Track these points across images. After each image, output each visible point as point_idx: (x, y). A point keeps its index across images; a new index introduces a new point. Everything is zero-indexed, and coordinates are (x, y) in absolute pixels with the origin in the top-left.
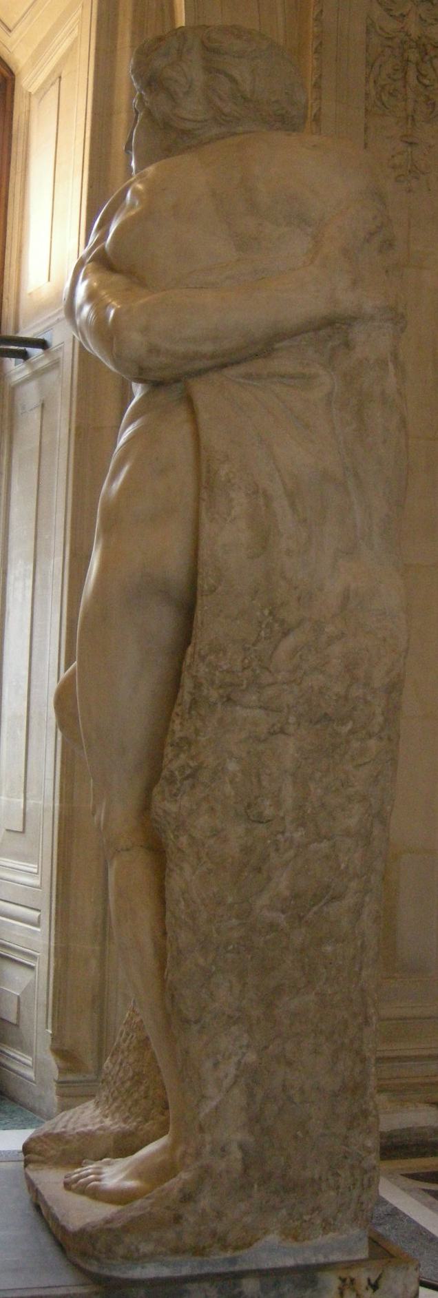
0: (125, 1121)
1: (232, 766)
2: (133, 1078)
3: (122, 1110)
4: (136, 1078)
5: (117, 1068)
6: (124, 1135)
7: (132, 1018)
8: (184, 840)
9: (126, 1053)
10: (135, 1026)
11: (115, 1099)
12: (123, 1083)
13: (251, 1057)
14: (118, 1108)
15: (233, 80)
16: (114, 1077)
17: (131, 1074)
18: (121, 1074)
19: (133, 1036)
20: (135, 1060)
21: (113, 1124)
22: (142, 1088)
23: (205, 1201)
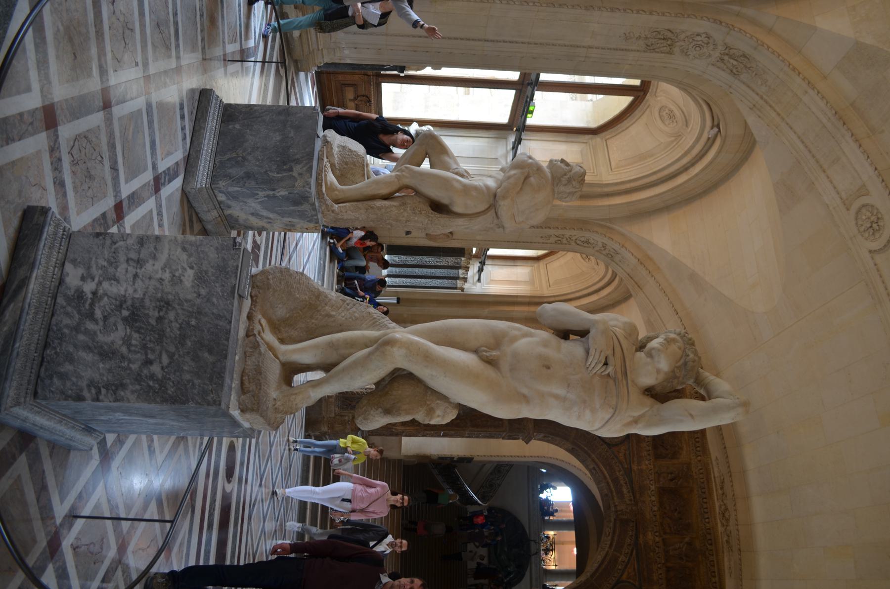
1: (416, 218)
6: (335, 166)
8: (402, 211)
13: (361, 219)
15: (566, 198)
21: (336, 160)
22: (345, 166)
23: (333, 214)
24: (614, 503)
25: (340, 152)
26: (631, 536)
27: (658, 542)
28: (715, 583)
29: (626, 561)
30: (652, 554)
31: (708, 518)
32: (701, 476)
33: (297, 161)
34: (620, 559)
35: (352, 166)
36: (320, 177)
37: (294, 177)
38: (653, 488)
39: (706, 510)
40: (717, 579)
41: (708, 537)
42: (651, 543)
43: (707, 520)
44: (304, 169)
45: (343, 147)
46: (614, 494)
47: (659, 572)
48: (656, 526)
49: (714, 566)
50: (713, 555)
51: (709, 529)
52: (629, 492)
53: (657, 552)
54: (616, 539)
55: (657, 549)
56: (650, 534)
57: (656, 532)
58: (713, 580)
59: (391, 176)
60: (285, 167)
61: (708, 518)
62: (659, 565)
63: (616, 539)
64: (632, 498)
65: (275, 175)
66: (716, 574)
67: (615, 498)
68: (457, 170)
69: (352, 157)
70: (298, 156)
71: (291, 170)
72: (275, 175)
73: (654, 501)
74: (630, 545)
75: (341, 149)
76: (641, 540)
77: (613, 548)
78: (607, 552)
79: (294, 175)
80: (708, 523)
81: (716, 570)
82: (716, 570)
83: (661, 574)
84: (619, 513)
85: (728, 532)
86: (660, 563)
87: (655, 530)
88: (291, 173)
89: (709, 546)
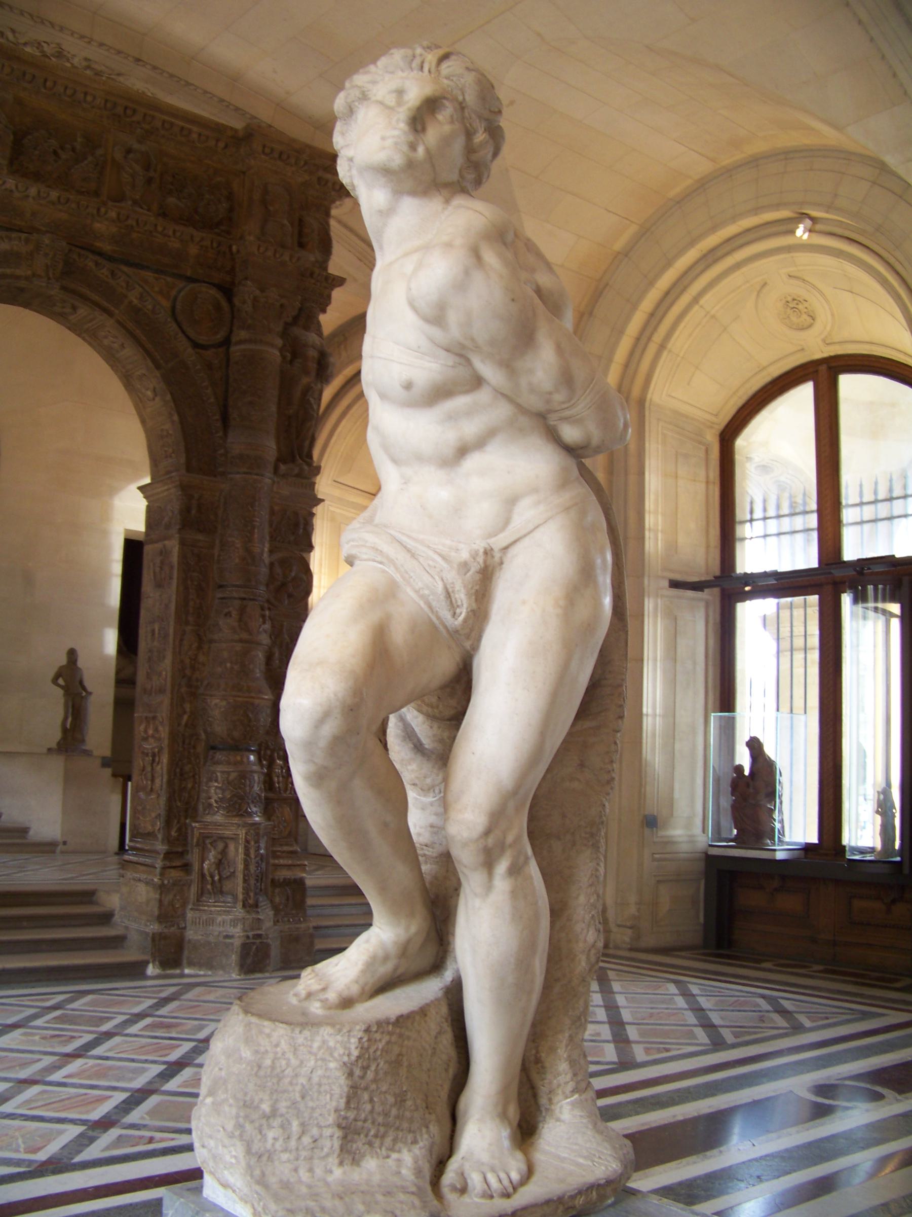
0: (415, 1142)
2: (396, 1101)
3: (402, 1138)
4: (399, 1099)
5: (368, 1107)
7: (368, 1049)
9: (374, 1086)
10: (379, 1053)
11: (383, 1137)
12: (386, 1114)
14: (395, 1140)
16: (370, 1117)
17: (391, 1099)
18: (378, 1108)
19: (378, 1065)
20: (391, 1084)
22: (409, 1103)
24: (27, 278)
25: (370, 1144)
26: (97, 264)
27: (119, 214)
28: (200, 135)
29: (141, 289)
30: (134, 235)
34: (136, 302)
35: (403, 1071)
38: (11, 183)
39: (69, 92)
40: (195, 129)
41: (120, 110)
42: (114, 230)
45: (345, 1137)
46: (8, 271)
47: (171, 233)
48: (87, 207)
49: (172, 124)
50: (153, 117)
51: (106, 101)
52: (10, 239)
53: (134, 224)
54: (95, 297)
55: (130, 222)
56: (97, 225)
57: (98, 210)
59: (514, 894)
62: (160, 229)
63: (95, 297)
64: (23, 236)
67: (18, 272)
68: (462, 597)
69: (375, 1081)
73: (39, 192)
74: (113, 273)
75: (359, 1144)
76: (107, 248)
77: (113, 309)
78: (119, 322)
81: (181, 124)
82: (181, 124)
83: (174, 232)
84: (51, 276)
86: (156, 226)
87: (95, 212)
89: (135, 119)
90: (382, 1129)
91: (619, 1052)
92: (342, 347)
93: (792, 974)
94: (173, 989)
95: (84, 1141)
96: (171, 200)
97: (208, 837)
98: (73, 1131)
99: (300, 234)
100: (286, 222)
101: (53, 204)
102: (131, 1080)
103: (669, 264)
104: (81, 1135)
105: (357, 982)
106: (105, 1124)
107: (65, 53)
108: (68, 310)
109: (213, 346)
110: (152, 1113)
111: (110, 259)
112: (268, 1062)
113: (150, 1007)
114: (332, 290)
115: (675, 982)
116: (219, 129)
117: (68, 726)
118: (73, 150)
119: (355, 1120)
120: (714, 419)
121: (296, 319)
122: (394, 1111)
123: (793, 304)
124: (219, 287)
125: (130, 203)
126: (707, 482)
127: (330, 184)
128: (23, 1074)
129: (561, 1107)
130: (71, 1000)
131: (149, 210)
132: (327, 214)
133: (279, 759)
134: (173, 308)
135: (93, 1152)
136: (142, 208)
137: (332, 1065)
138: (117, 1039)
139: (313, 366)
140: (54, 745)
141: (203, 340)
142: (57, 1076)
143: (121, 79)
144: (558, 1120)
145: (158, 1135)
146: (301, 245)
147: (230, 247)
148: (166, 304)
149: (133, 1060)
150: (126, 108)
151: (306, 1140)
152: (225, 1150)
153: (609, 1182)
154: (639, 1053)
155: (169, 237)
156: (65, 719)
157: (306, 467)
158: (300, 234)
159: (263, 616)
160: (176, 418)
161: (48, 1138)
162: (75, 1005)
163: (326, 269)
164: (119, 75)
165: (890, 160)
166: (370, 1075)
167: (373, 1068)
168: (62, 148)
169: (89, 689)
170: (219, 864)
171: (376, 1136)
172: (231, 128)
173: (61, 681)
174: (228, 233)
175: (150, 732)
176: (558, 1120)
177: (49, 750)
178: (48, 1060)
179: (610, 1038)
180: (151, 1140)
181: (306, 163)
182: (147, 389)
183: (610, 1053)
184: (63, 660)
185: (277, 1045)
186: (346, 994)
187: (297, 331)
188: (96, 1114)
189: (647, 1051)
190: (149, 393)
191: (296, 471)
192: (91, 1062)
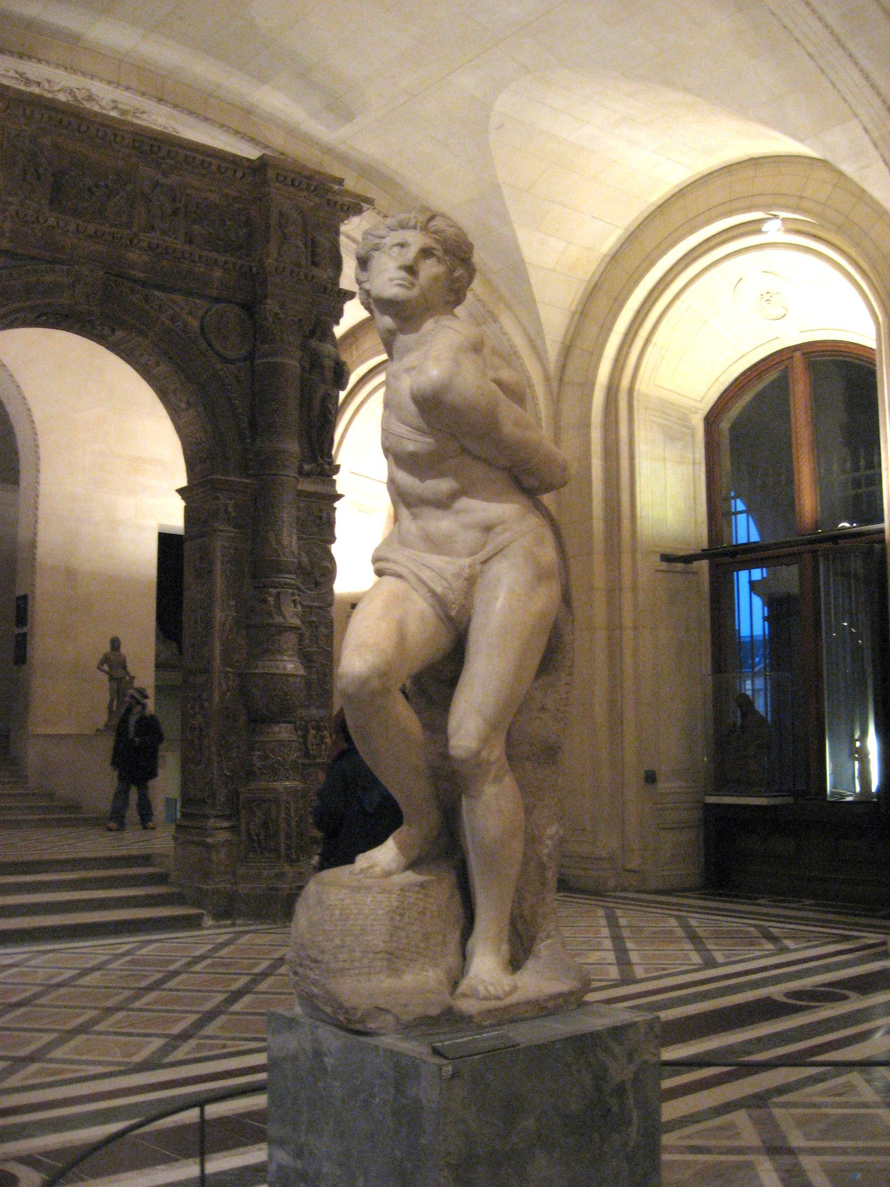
0: (437, 966)
9: (407, 928)
25: (408, 965)
31: (115, 136)
32: (37, 116)
33: (600, 1077)
36: (551, 1004)
37: (636, 1073)
41: (146, 148)
43: (119, 139)
44: (617, 1049)
49: (194, 158)
55: (159, 250)
57: (131, 241)
58: (214, 168)
60: (615, 1109)
61: (115, 136)
64: (66, 267)
65: (633, 1129)
66: (208, 159)
70: (588, 1081)
71: (620, 1090)
72: (633, 1129)
79: (632, 1076)
80: (123, 138)
81: (201, 158)
82: (201, 158)
83: (200, 257)
85: (113, 105)
88: (628, 1085)
89: (161, 154)
90: (415, 956)
91: (621, 972)
92: (354, 346)
93: (786, 908)
94: (226, 937)
95: (165, 1050)
96: (196, 228)
97: (254, 801)
98: (159, 1042)
99: (314, 254)
100: (300, 243)
101: (90, 236)
102: (200, 1004)
103: (652, 263)
104: (166, 1045)
105: (394, 861)
106: (184, 1036)
107: (94, 97)
108: (107, 331)
109: (239, 360)
110: (221, 1028)
111: (144, 284)
112: (337, 912)
113: (210, 950)
114: (344, 303)
115: (676, 917)
116: (235, 161)
117: (114, 708)
118: (106, 186)
119: (397, 948)
120: (698, 405)
121: (313, 333)
122: (422, 945)
123: (768, 298)
124: (245, 306)
125: (158, 233)
126: (694, 463)
127: (338, 206)
128: (109, 1004)
129: (539, 949)
130: (139, 948)
131: (176, 238)
132: (337, 233)
133: (313, 728)
134: (202, 328)
135: (179, 1054)
136: (170, 237)
137: (380, 912)
138: (184, 976)
139: (329, 375)
140: (101, 726)
141: (231, 354)
142: (137, 1004)
143: (144, 116)
144: (538, 957)
145: (229, 1043)
146: (314, 263)
147: (251, 268)
148: (195, 324)
149: (200, 991)
150: (152, 146)
151: (366, 961)
152: (311, 972)
153: (571, 993)
154: (639, 972)
155: (195, 262)
156: (112, 701)
157: (327, 467)
158: (314, 254)
159: (294, 601)
160: (209, 428)
161: (139, 1047)
162: (144, 951)
163: (337, 284)
164: (143, 112)
165: (847, 168)
166: (406, 919)
167: (407, 915)
168: (97, 186)
169: (133, 674)
170: (265, 825)
171: (411, 960)
172: (248, 160)
173: (106, 667)
174: (249, 255)
175: (197, 709)
176: (538, 957)
177: (98, 730)
178: (127, 993)
179: (614, 961)
180: (224, 1046)
181: (315, 189)
182: (181, 401)
183: (614, 973)
184: (106, 648)
185: (343, 900)
186: (387, 869)
187: (314, 343)
188: (176, 1029)
189: (646, 971)
190: (183, 405)
191: (319, 470)
192: (164, 993)
